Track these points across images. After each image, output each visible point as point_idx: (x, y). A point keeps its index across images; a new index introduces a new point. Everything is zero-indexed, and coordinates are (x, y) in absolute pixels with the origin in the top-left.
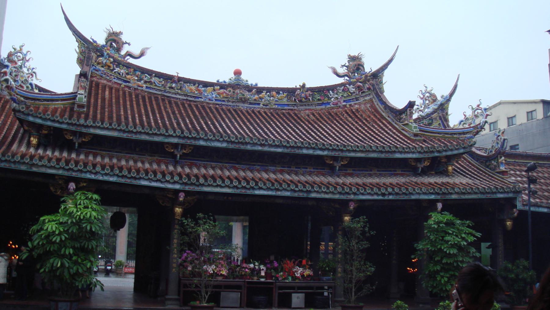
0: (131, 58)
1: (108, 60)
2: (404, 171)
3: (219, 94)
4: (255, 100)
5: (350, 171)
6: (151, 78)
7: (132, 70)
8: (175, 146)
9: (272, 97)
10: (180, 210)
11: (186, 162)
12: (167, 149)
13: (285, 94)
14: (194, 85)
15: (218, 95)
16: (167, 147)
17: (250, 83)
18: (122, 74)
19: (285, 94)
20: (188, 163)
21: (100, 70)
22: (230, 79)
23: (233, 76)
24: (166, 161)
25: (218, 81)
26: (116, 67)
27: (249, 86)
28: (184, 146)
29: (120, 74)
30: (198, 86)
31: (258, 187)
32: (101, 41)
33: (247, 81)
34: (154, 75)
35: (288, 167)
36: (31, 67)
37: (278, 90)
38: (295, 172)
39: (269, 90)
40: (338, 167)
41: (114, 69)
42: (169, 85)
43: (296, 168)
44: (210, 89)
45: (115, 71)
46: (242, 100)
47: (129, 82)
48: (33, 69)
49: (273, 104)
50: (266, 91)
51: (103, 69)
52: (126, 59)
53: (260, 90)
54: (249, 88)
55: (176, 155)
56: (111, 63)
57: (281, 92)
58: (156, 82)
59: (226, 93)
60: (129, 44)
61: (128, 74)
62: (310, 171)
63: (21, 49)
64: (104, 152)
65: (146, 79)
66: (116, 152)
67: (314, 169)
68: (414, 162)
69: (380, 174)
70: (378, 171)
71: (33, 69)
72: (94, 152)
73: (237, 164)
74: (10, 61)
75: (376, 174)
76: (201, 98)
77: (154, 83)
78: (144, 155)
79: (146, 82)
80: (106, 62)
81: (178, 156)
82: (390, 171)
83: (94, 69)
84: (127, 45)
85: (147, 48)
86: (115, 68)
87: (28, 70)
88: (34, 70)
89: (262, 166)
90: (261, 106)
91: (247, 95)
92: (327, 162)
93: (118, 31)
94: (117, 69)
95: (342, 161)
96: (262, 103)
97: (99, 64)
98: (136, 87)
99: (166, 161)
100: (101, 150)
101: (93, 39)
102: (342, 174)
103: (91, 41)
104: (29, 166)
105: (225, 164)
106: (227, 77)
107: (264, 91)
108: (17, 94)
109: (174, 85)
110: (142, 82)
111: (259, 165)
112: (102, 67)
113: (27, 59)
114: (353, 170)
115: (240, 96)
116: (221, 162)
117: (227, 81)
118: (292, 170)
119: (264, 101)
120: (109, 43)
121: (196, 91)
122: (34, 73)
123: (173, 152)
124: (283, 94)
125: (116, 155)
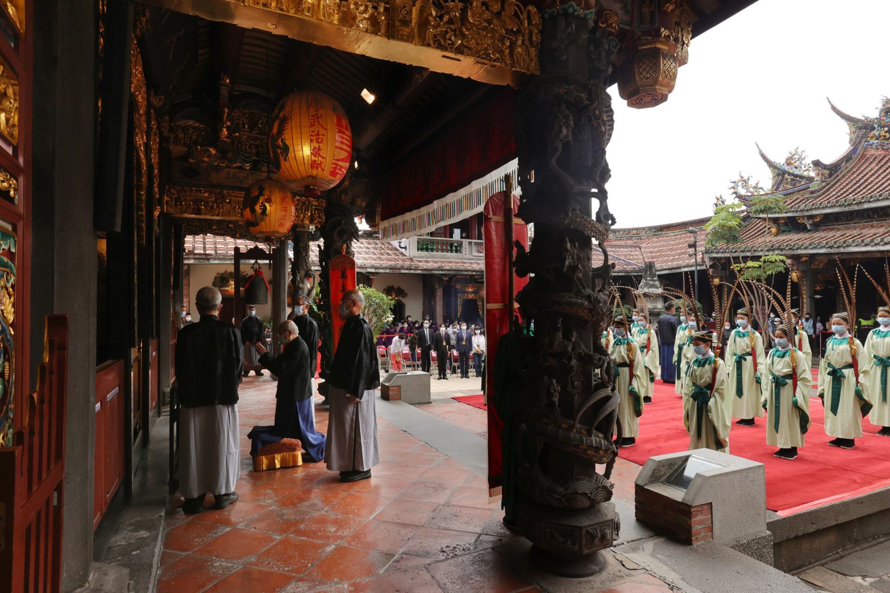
21: (873, 143)
36: (807, 163)
51: (877, 141)
56: (885, 133)
64: (841, 226)
66: (855, 223)
74: (789, 164)
78: (886, 220)
80: (879, 134)
97: (872, 138)
100: (838, 225)
101: (865, 117)
103: (863, 119)
108: (747, 200)
112: (877, 139)
113: (803, 157)
120: (883, 114)
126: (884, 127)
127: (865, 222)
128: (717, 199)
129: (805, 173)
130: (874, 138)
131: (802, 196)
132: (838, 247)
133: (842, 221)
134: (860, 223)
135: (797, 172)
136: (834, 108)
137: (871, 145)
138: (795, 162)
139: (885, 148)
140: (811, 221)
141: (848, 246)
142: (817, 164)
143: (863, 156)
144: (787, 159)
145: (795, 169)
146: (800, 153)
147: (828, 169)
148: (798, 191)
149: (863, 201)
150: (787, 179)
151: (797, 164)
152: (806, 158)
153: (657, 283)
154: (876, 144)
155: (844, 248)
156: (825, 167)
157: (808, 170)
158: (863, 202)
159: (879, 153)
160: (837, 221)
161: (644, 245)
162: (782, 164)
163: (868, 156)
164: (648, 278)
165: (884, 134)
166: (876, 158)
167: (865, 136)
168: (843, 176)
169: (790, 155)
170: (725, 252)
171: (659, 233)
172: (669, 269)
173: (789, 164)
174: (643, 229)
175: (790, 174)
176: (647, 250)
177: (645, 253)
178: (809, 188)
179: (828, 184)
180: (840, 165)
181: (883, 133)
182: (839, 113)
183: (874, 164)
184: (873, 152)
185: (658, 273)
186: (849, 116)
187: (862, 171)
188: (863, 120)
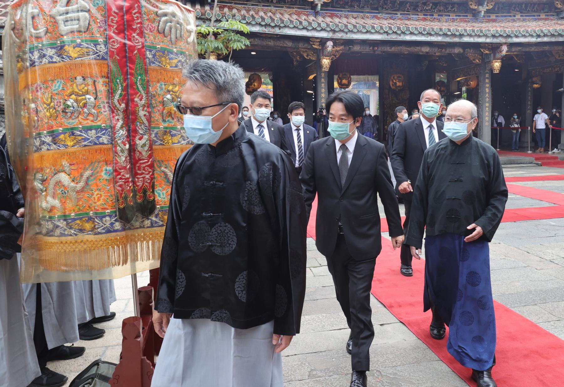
2: (548, 15)
5: (493, 17)
10: (328, 61)
24: (305, 13)
35: (430, 15)
38: (437, 19)
40: (483, 12)
43: (439, 15)
55: (317, 5)
62: (453, 19)
64: (240, 6)
66: (253, 5)
67: (456, 16)
68: (561, 4)
69: (523, 19)
70: (522, 16)
72: (228, 6)
73: (379, 13)
75: (519, 19)
78: (282, 7)
81: (319, 5)
82: (534, 16)
92: (471, 7)
95: (487, 6)
99: (305, 13)
100: (235, 3)
102: (485, 20)
105: (367, 14)
111: (401, 14)
114: (497, 16)
116: (362, 12)
118: (435, 18)
127: (263, 6)
134: (257, 5)
155: (280, 29)
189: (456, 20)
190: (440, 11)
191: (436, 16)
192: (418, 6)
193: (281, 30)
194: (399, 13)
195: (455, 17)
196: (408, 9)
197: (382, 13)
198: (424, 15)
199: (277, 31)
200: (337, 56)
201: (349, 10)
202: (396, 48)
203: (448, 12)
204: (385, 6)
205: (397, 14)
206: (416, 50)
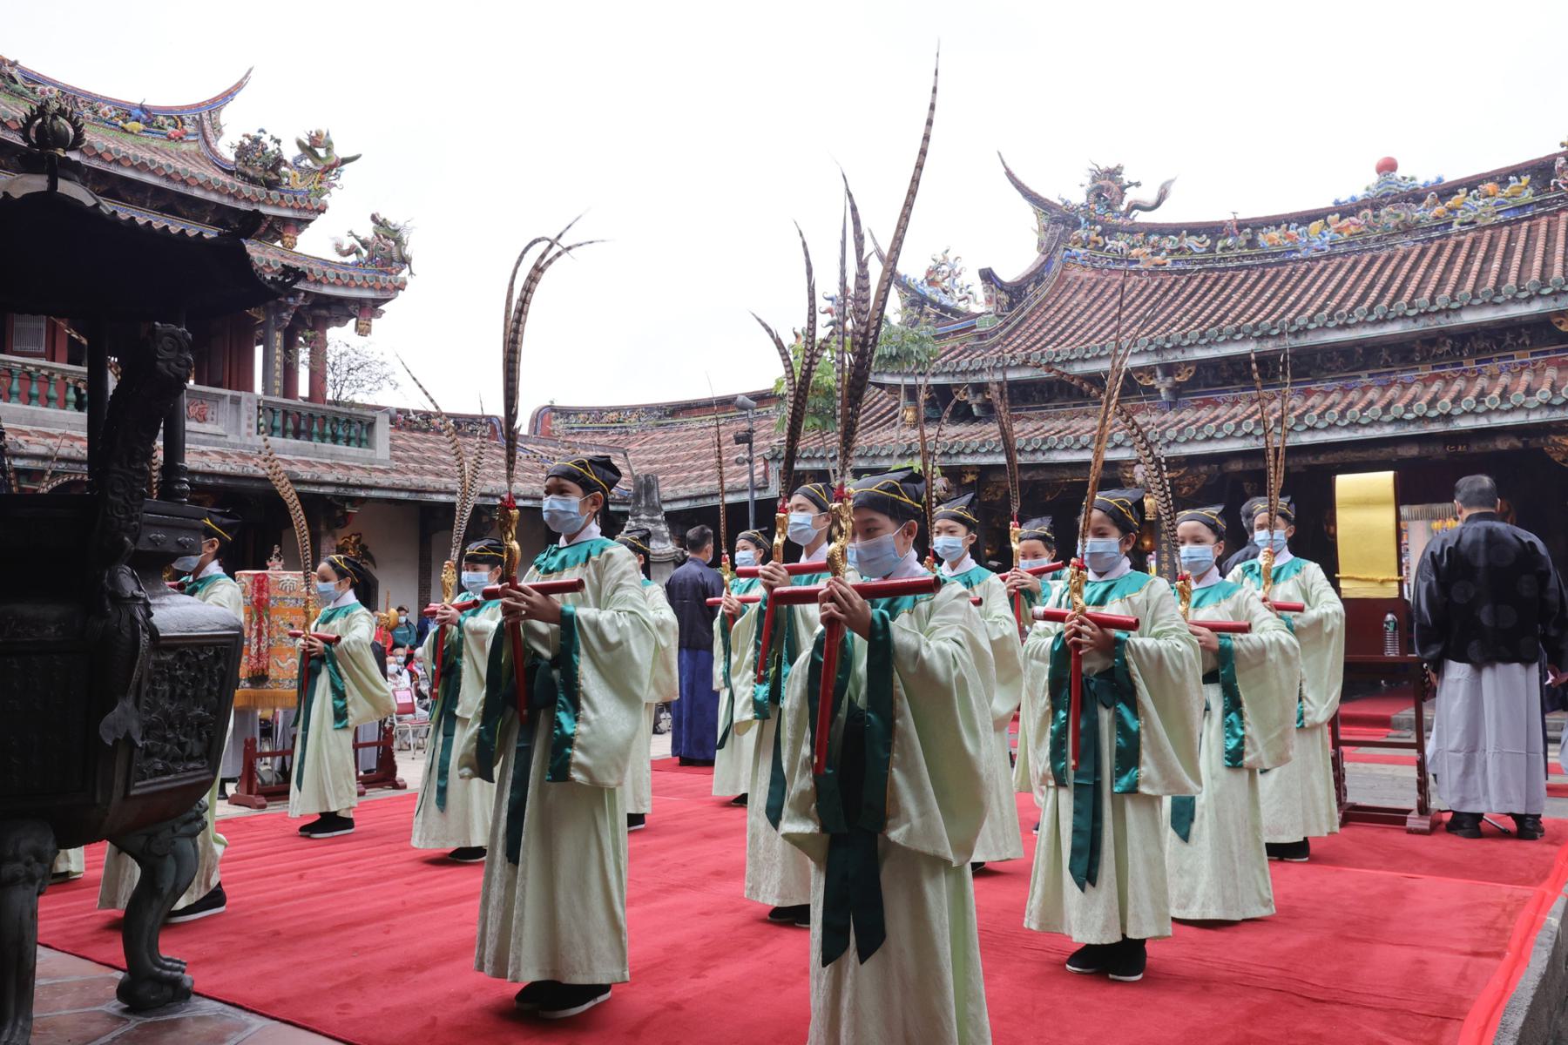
0: (1141, 213)
1: (1091, 230)
3: (1339, 231)
4: (1437, 218)
6: (1180, 241)
7: (1140, 236)
8: (1150, 371)
9: (1488, 196)
11: (1194, 401)
12: (1141, 382)
13: (1523, 178)
14: (1278, 226)
15: (1338, 233)
16: (1140, 378)
17: (1420, 182)
18: (1122, 250)
19: (1523, 178)
20: (1198, 402)
21: (1078, 255)
22: (1367, 189)
23: (1373, 178)
25: (1337, 202)
26: (1110, 240)
27: (1417, 189)
28: (1169, 369)
29: (1116, 251)
30: (1288, 229)
31: (1305, 427)
32: (1078, 197)
33: (1412, 179)
34: (1185, 232)
35: (1454, 365)
36: (965, 285)
37: (1502, 177)
38: (1474, 372)
39: (1472, 184)
41: (1106, 245)
42: (1220, 244)
44: (1316, 226)
45: (1107, 247)
46: (1399, 229)
47: (1138, 262)
48: (968, 287)
49: (1489, 214)
50: (1465, 189)
51: (1084, 251)
52: (1131, 217)
53: (1446, 192)
54: (1416, 196)
56: (1097, 235)
57: (1511, 178)
58: (1193, 247)
59: (1355, 224)
60: (1138, 184)
61: (1133, 247)
63: (945, 258)
64: (1033, 412)
65: (1169, 246)
66: (1056, 407)
71: (968, 287)
73: (1314, 382)
74: (932, 283)
76: (1297, 251)
77: (1190, 248)
79: (1172, 252)
80: (1087, 237)
83: (1068, 256)
84: (1133, 187)
85: (1170, 182)
86: (1107, 241)
87: (961, 291)
88: (970, 289)
89: (1380, 374)
90: (1456, 226)
91: (1418, 213)
93: (1112, 166)
94: (1111, 244)
96: (1456, 221)
98: (1151, 267)
100: (1028, 409)
101: (1062, 200)
103: (1060, 203)
104: (870, 461)
106: (1358, 182)
107: (1460, 191)
109: (1230, 241)
110: (1164, 254)
111: (1370, 376)
112: (1084, 247)
113: (957, 271)
115: (1392, 222)
116: (1274, 386)
117: (1360, 193)
118: (1465, 370)
119: (1462, 214)
120: (1092, 197)
121: (1285, 239)
122: (970, 293)
123: (1153, 386)
124: (1520, 181)
125: (1055, 413)
126: (1094, 223)
127: (1075, 406)
128: (797, 336)
129: (962, 305)
130: (1080, 245)
131: (961, 344)
132: (1034, 451)
133: (1034, 402)
134: (1064, 406)
135: (946, 301)
136: (1009, 174)
137: (1074, 258)
138: (943, 280)
139: (1097, 265)
140: (979, 399)
141: (1050, 449)
142: (987, 276)
143: (1062, 279)
144: (929, 273)
145: (942, 294)
146: (951, 261)
147: (1006, 292)
148: (955, 333)
149: (1073, 357)
150: (928, 315)
151: (945, 284)
152: (963, 272)
153: (663, 528)
154: (1082, 257)
155: (1044, 454)
156: (1002, 286)
157: (966, 298)
158: (1073, 361)
159: (1088, 275)
160: (1026, 401)
161: (634, 447)
162: (919, 281)
163: (1069, 279)
164: (643, 517)
165: (1096, 238)
166: (1082, 283)
167: (1063, 239)
168: (1032, 313)
169: (933, 264)
170: (814, 458)
171: (669, 420)
172: (690, 498)
173: (932, 283)
174: (633, 409)
175: (934, 304)
176: (642, 457)
177: (635, 462)
178: (975, 327)
179: (1007, 324)
180: (1025, 288)
181: (1093, 236)
182: (1020, 186)
183: (1080, 296)
184: (1077, 272)
185: (666, 507)
186: (1036, 194)
187: (1063, 306)
188: (1061, 207)
189: (1534, 364)
190: (1479, 351)
191: (1470, 364)
192: (1412, 351)
193: (1047, 455)
194: (1364, 374)
195: (1530, 359)
196: (1387, 361)
197: (1323, 380)
198: (1433, 368)
199: (1040, 458)
200: (1197, 487)
201: (1243, 386)
202: (1330, 456)
203: (1505, 349)
204: (1329, 365)
205: (1359, 377)
206: (1381, 455)
